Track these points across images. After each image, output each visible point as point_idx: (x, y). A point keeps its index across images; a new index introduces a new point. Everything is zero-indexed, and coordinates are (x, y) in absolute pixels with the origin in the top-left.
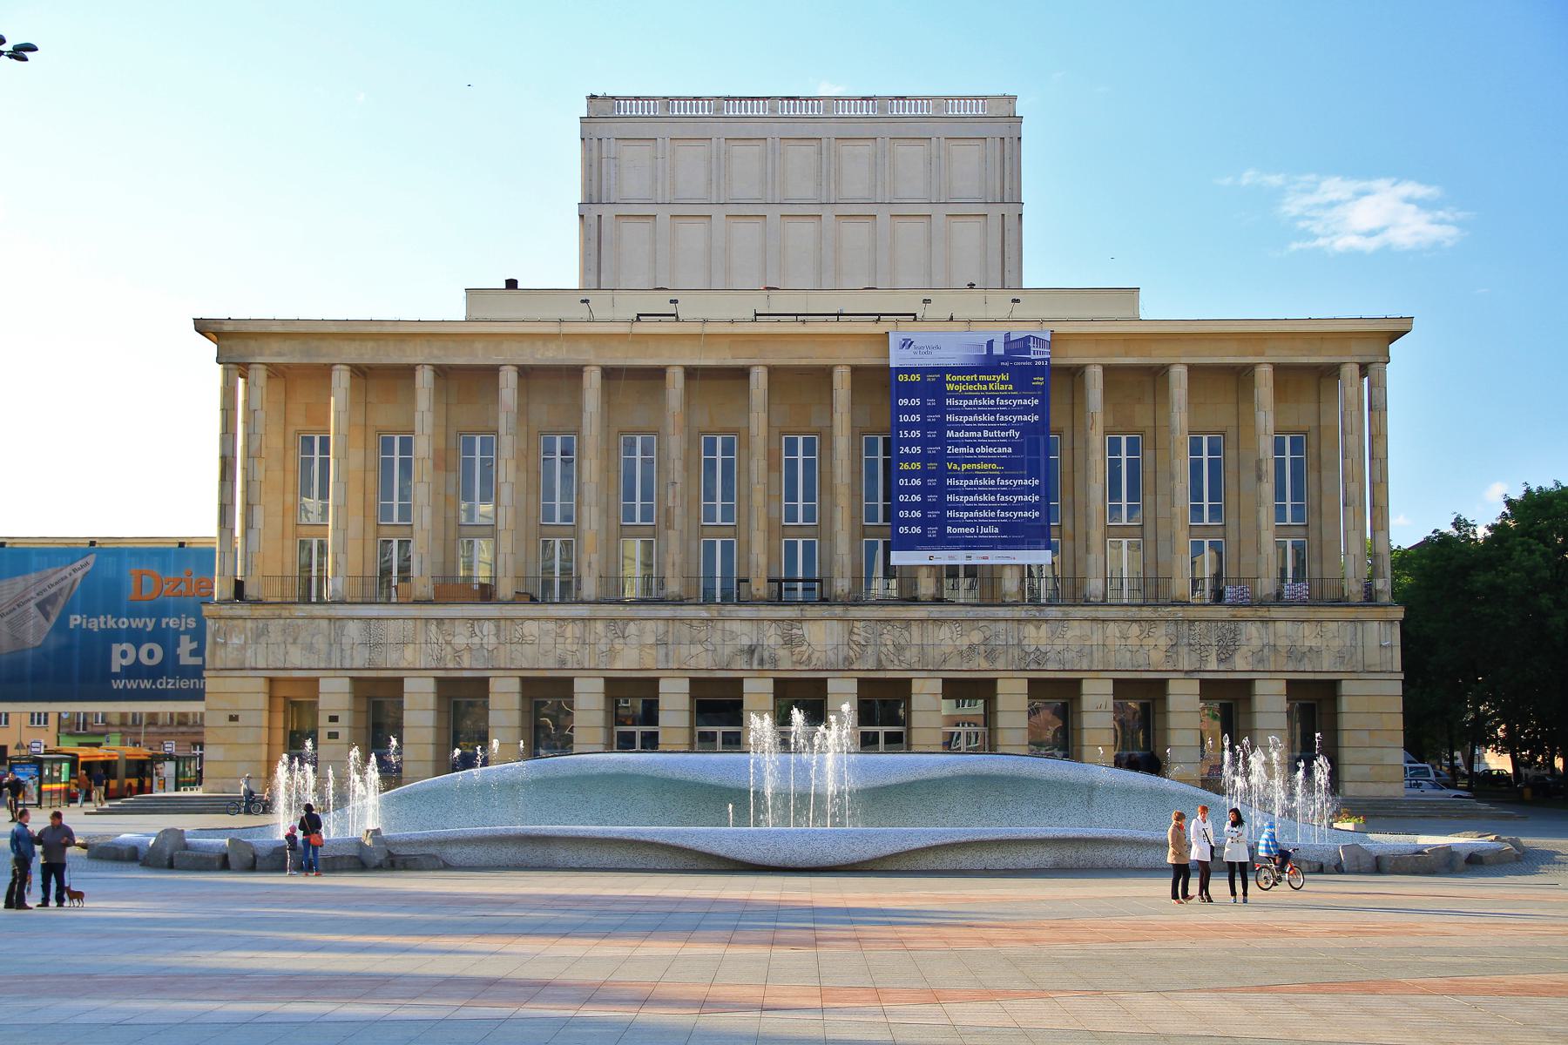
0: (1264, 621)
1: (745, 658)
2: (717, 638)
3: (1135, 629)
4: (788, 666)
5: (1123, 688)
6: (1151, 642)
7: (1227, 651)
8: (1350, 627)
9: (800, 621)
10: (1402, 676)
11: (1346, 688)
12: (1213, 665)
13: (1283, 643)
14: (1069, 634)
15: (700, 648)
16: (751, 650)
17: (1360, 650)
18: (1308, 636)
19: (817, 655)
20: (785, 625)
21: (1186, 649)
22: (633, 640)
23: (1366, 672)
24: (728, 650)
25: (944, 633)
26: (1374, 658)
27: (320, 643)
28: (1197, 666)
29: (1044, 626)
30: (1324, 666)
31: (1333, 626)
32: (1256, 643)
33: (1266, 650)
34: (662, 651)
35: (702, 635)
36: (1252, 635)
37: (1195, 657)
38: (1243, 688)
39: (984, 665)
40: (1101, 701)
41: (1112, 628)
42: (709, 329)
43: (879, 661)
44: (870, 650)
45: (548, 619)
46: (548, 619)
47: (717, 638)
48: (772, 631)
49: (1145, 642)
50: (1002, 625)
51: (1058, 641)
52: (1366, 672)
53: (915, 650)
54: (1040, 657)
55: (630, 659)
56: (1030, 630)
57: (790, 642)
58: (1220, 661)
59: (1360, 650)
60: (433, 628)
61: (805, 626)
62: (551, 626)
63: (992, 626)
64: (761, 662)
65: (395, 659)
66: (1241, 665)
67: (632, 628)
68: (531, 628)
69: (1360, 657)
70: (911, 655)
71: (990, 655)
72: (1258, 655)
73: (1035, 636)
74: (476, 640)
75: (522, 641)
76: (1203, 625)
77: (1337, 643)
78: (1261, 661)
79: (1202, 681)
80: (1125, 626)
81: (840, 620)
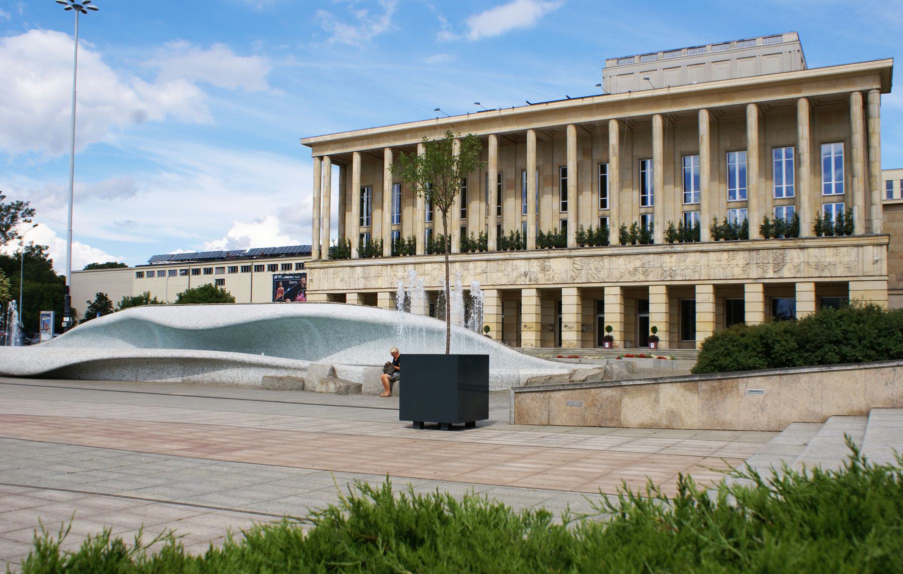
0: (802, 248)
1: (523, 278)
2: (509, 269)
5: (719, 290)
6: (735, 262)
7: (779, 266)
8: (855, 249)
11: (852, 286)
12: (770, 274)
13: (813, 260)
14: (688, 260)
15: (501, 274)
16: (526, 274)
17: (860, 263)
18: (828, 256)
20: (541, 261)
21: (755, 266)
22: (472, 272)
23: (866, 277)
24: (515, 274)
25: (621, 260)
26: (870, 269)
27: (346, 277)
28: (760, 275)
29: (675, 256)
30: (837, 274)
31: (844, 249)
32: (796, 261)
33: (802, 265)
34: (484, 276)
35: (503, 268)
36: (794, 257)
37: (760, 270)
38: (789, 289)
39: (642, 278)
40: (706, 297)
42: (503, 113)
43: (588, 278)
44: (583, 272)
47: (509, 269)
49: (731, 262)
50: (652, 256)
51: (682, 264)
52: (866, 277)
53: (606, 271)
54: (672, 272)
56: (666, 258)
57: (544, 269)
58: (775, 272)
59: (860, 263)
61: (551, 260)
62: (436, 265)
63: (646, 257)
64: (530, 280)
66: (787, 274)
67: (471, 265)
69: (860, 267)
70: (603, 275)
71: (645, 273)
72: (797, 268)
73: (669, 261)
74: (406, 274)
75: (424, 274)
76: (765, 251)
77: (846, 259)
78: (799, 271)
80: (718, 254)
81: (568, 257)
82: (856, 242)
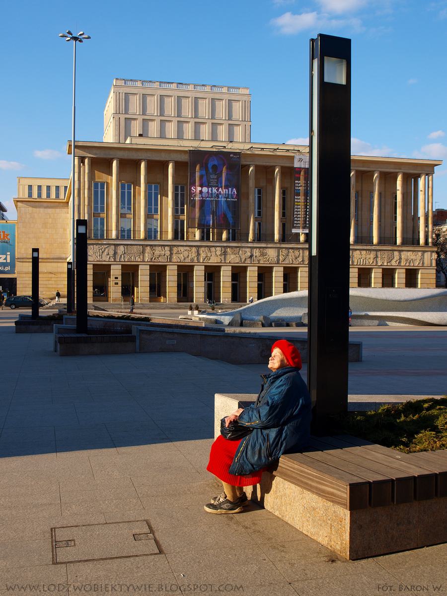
3: (364, 252)
4: (263, 263)
9: (266, 248)
10: (436, 268)
19: (271, 259)
41: (358, 252)
45: (186, 246)
46: (186, 246)
48: (257, 251)
55: (214, 260)
57: (263, 255)
60: (148, 248)
62: (188, 248)
65: (135, 259)
67: (213, 249)
68: (180, 248)
74: (163, 252)
79: (383, 269)
82: (424, 250)
